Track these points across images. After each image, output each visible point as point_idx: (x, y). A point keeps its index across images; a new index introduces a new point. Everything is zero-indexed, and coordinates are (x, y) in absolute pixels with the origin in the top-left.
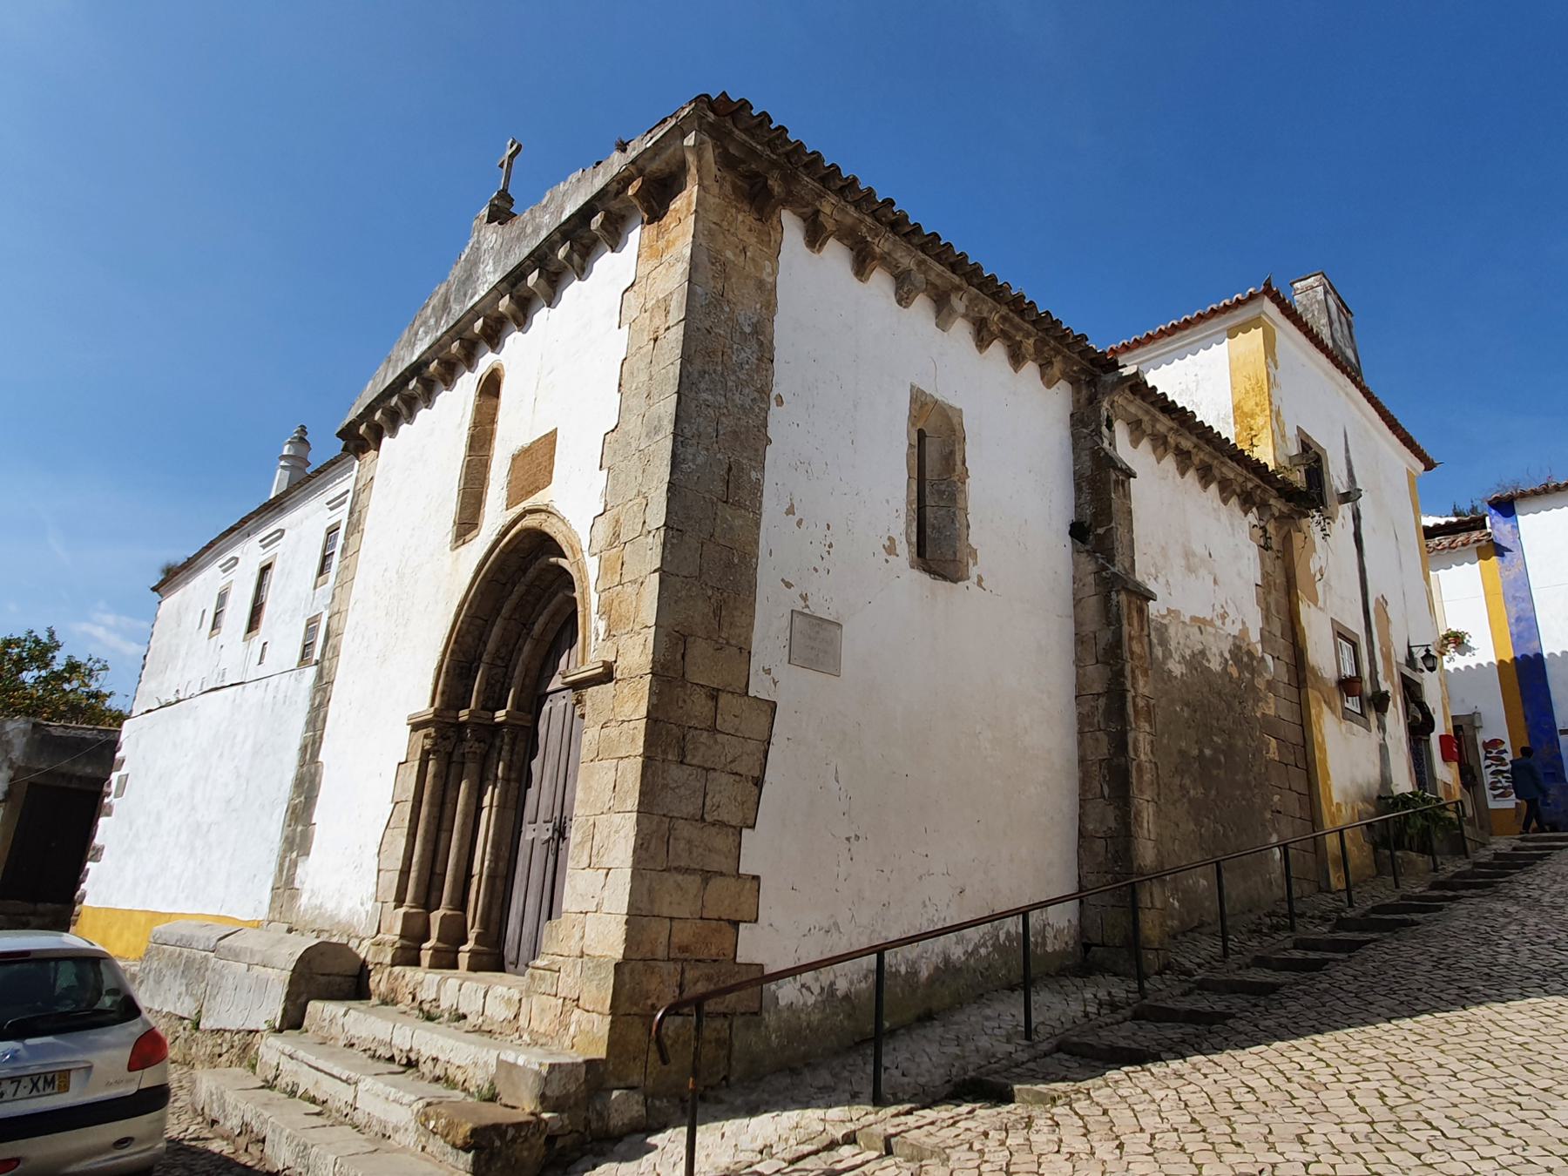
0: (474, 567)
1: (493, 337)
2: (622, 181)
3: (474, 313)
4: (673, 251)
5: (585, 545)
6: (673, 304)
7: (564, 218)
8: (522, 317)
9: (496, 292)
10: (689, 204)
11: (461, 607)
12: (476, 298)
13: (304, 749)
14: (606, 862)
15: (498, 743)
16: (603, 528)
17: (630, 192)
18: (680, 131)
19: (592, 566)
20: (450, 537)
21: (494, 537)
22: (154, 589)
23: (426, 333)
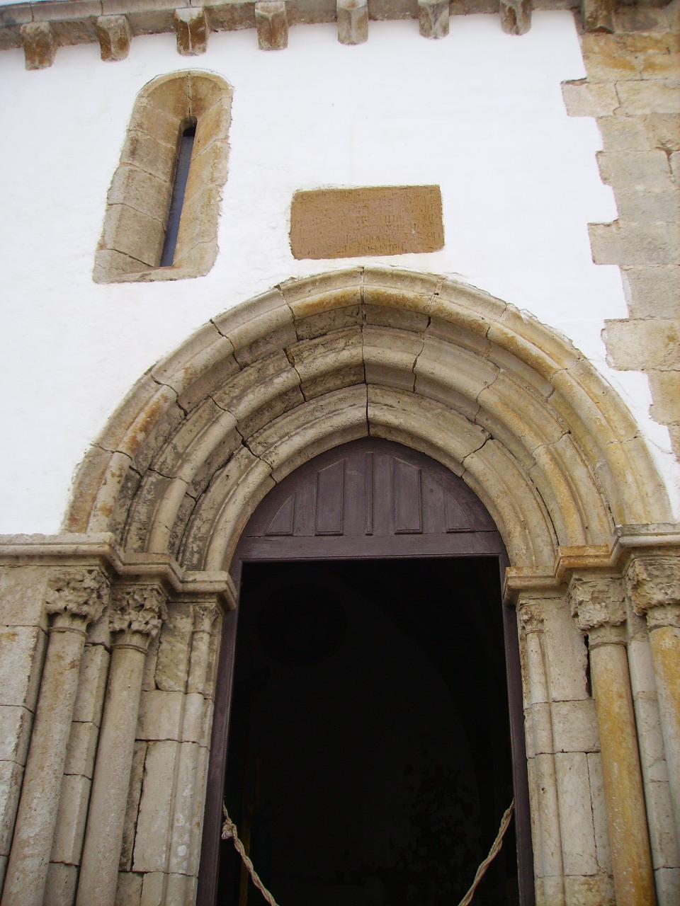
0: (199, 320)
15: (184, 624)
20: (89, 263)
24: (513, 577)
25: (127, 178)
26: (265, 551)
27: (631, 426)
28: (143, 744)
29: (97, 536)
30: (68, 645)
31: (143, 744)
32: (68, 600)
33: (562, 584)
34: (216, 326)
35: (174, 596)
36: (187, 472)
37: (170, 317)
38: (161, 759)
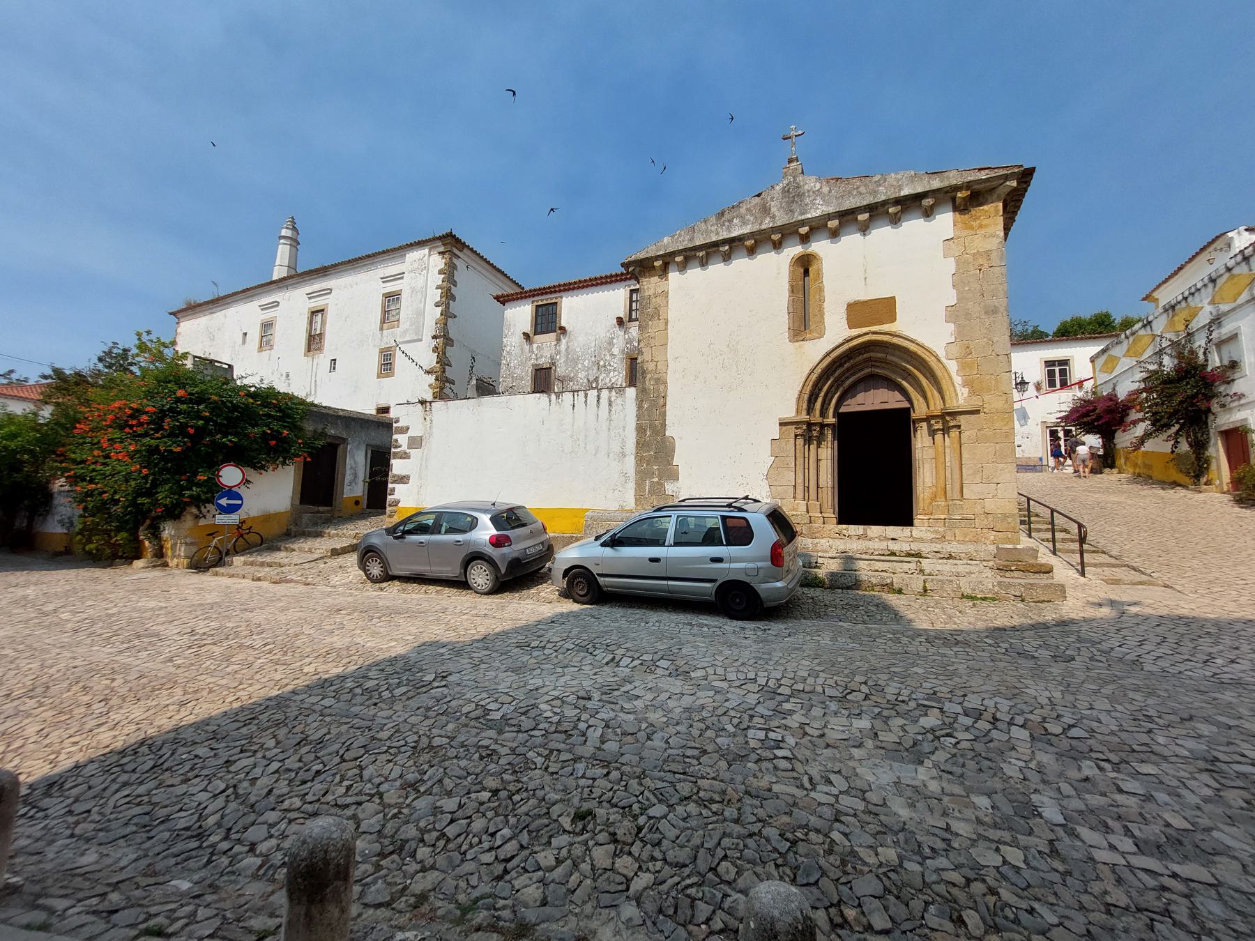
0: (823, 353)
1: (805, 239)
2: (956, 188)
3: (803, 223)
4: (990, 230)
5: (941, 354)
6: (994, 255)
7: (902, 193)
8: (835, 234)
9: (829, 217)
10: (997, 211)
11: (812, 371)
12: (809, 216)
13: (640, 430)
14: (995, 480)
16: (955, 350)
17: (959, 195)
18: (1006, 177)
19: (952, 366)
21: (841, 341)
22: (173, 314)
23: (744, 223)
24: (913, 416)
25: (792, 303)
26: (843, 410)
27: (950, 377)
28: (818, 461)
29: (804, 417)
30: (800, 442)
31: (818, 461)
32: (799, 432)
33: (927, 419)
34: (828, 354)
35: (822, 426)
36: (822, 394)
37: (815, 352)
38: (823, 464)
